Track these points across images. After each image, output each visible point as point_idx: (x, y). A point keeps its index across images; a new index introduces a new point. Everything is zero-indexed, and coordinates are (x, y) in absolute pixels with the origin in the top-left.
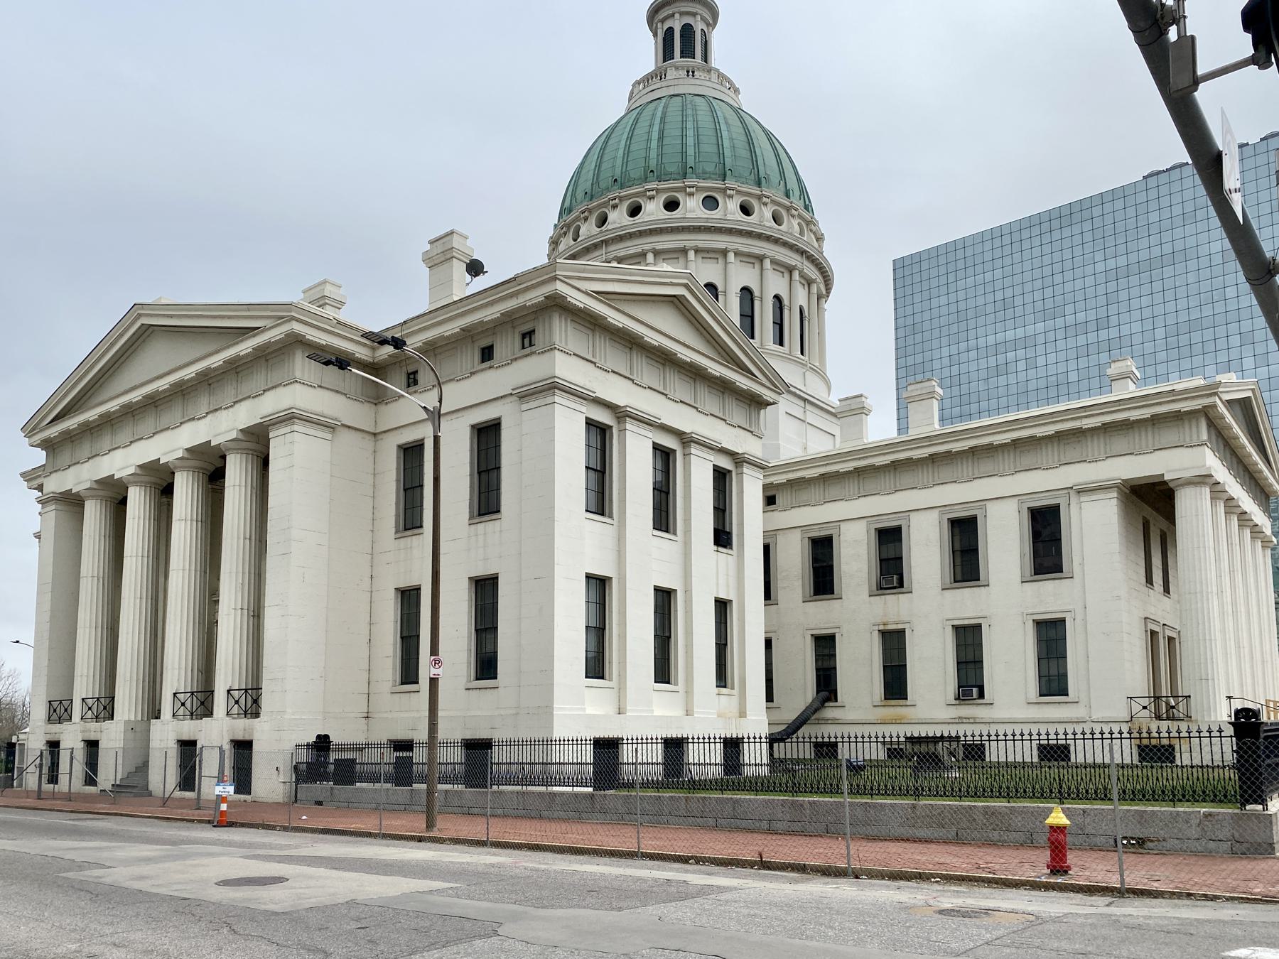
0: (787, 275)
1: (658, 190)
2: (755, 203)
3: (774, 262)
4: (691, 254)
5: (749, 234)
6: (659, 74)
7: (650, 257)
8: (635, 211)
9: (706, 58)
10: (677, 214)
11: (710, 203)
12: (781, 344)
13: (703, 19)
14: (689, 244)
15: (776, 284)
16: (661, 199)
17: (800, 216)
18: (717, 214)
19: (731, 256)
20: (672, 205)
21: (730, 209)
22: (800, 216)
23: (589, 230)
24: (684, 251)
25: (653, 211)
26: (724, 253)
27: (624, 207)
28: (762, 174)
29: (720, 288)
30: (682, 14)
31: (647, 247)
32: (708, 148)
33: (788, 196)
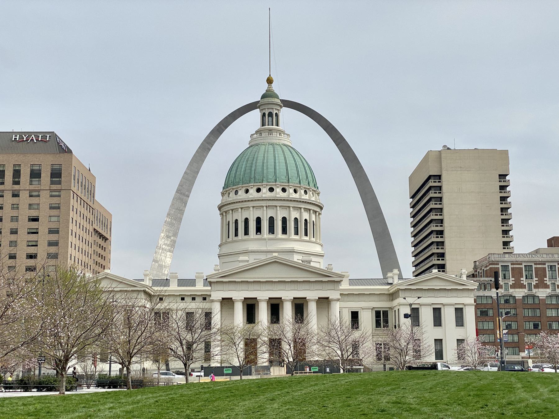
2: (287, 188)
5: (284, 200)
6: (259, 132)
7: (251, 208)
8: (247, 191)
11: (271, 190)
15: (295, 214)
16: (255, 188)
17: (305, 188)
19: (278, 207)
20: (259, 190)
23: (233, 197)
24: (263, 207)
25: (253, 191)
26: (276, 206)
27: (244, 189)
31: (249, 206)
32: (271, 170)
33: (300, 182)
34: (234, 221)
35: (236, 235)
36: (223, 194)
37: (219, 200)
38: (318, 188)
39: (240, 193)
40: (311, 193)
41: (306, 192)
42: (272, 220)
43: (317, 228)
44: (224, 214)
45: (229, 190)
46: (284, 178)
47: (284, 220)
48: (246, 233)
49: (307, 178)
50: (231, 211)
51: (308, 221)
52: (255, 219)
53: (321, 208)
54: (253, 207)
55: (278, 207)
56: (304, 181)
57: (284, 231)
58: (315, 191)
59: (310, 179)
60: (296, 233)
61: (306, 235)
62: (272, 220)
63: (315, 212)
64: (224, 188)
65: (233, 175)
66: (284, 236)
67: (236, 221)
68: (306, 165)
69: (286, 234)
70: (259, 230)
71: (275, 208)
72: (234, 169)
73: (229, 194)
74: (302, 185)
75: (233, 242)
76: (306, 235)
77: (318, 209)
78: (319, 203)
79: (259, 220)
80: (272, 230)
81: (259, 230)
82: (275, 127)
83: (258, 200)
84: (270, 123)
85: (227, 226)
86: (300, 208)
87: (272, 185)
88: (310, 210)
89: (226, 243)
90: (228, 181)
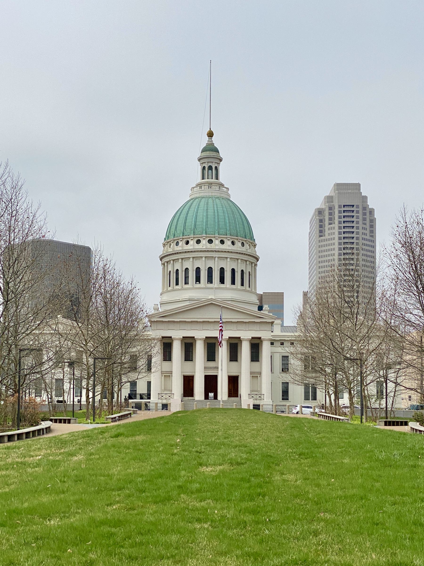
0: (236, 261)
1: (194, 237)
2: (225, 240)
3: (231, 258)
4: (204, 258)
6: (199, 185)
8: (187, 243)
9: (217, 178)
11: (210, 241)
13: (215, 163)
19: (216, 258)
20: (198, 242)
24: (202, 257)
27: (184, 241)
28: (228, 228)
30: (208, 162)
34: (175, 271)
35: (177, 284)
36: (164, 245)
37: (161, 251)
38: (254, 240)
39: (180, 243)
41: (243, 244)
42: (210, 270)
43: (252, 277)
44: (166, 264)
45: (170, 241)
47: (222, 270)
48: (186, 283)
50: (172, 262)
51: (245, 272)
52: (195, 269)
53: (258, 260)
54: (193, 258)
56: (242, 233)
57: (222, 281)
58: (252, 243)
61: (242, 284)
62: (210, 270)
64: (165, 239)
65: (173, 227)
66: (222, 286)
67: (177, 270)
68: (244, 219)
70: (198, 279)
72: (175, 221)
73: (171, 245)
75: (173, 290)
76: (242, 284)
79: (198, 270)
80: (210, 280)
81: (198, 279)
82: (214, 180)
84: (210, 176)
85: (168, 276)
87: (211, 237)
88: (246, 261)
89: (168, 291)
90: (170, 232)
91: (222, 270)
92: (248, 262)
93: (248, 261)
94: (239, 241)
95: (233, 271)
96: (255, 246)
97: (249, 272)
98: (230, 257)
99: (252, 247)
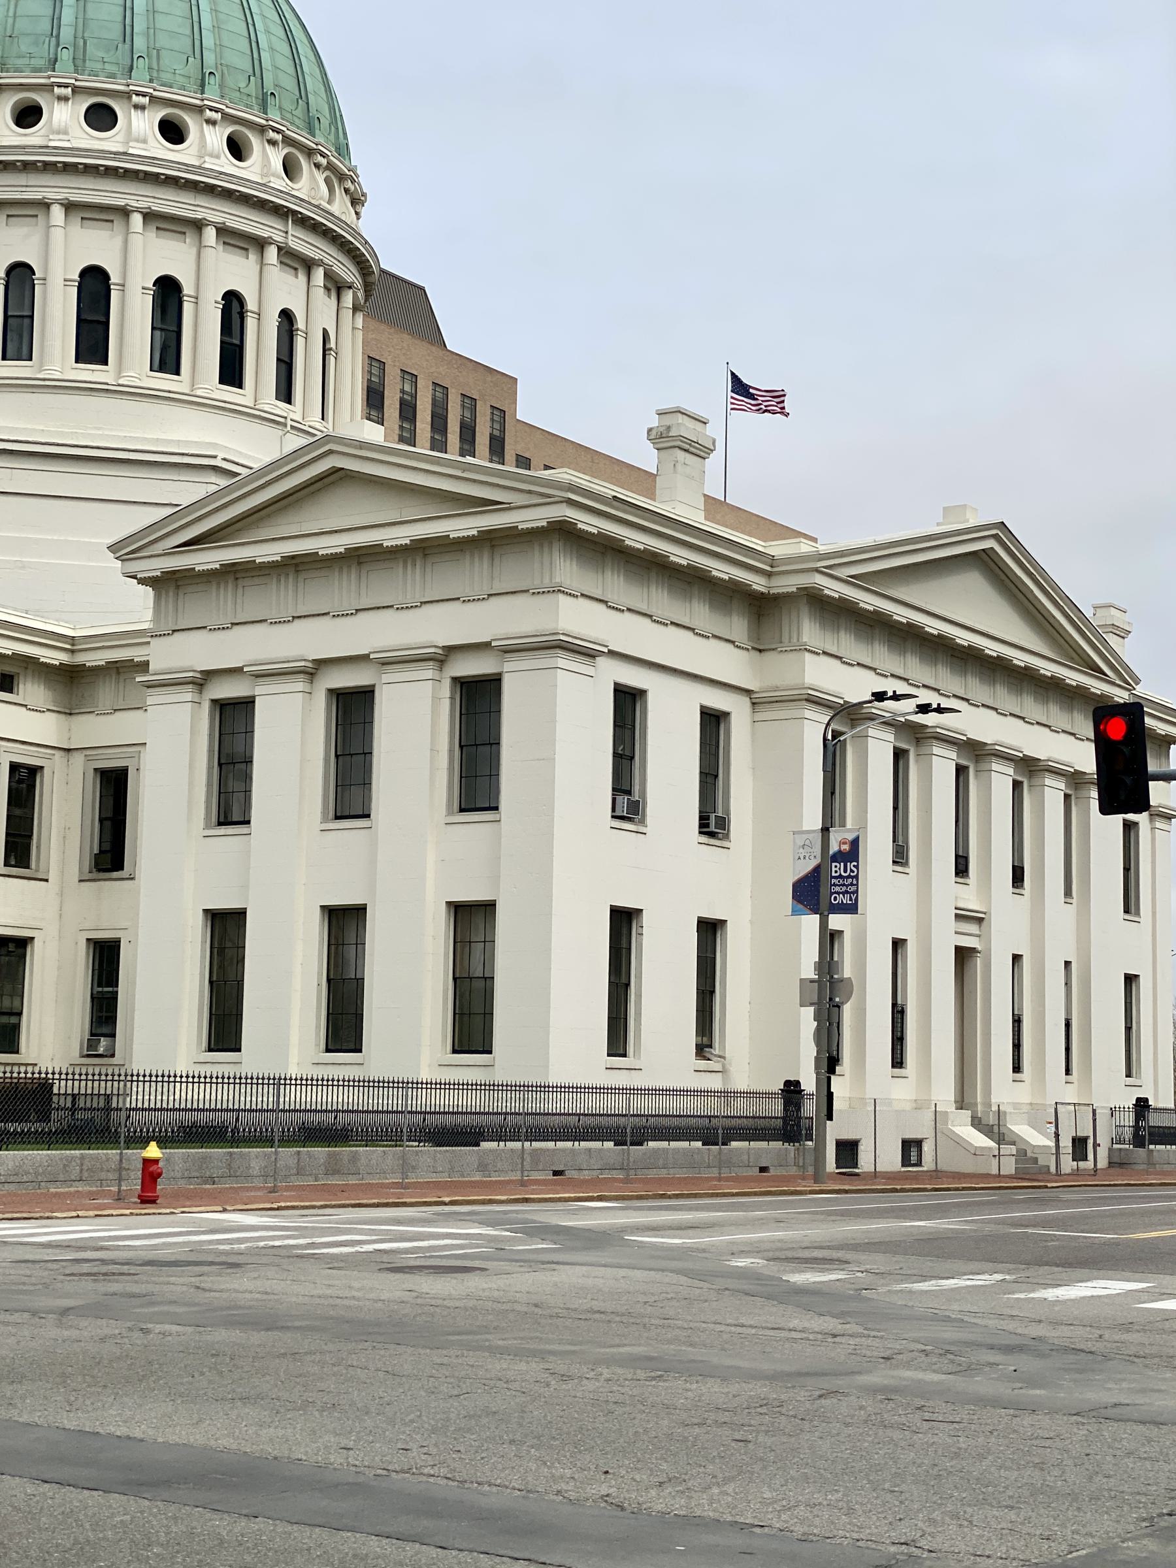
0: (253, 257)
2: (191, 123)
3: (223, 231)
10: (34, 136)
11: (101, 117)
12: (239, 384)
14: (50, 195)
17: (288, 141)
18: (109, 141)
21: (137, 134)
22: (288, 141)
24: (45, 205)
26: (125, 212)
29: (114, 279)
40: (320, 177)
41: (290, 169)
42: (94, 286)
46: (175, 64)
47: (168, 293)
49: (302, 94)
51: (300, 324)
55: (137, 220)
59: (318, 102)
60: (232, 370)
61: (285, 392)
62: (94, 286)
63: (336, 286)
66: (164, 382)
69: (178, 373)
71: (118, 223)
74: (274, 114)
76: (285, 392)
77: (347, 272)
78: (357, 234)
80: (92, 343)
83: (27, 167)
86: (260, 244)
88: (308, 265)
91: (168, 293)
92: (319, 275)
93: (320, 263)
94: (273, 143)
95: (233, 304)
96: (356, 201)
97: (325, 334)
98: (217, 218)
99: (340, 197)
